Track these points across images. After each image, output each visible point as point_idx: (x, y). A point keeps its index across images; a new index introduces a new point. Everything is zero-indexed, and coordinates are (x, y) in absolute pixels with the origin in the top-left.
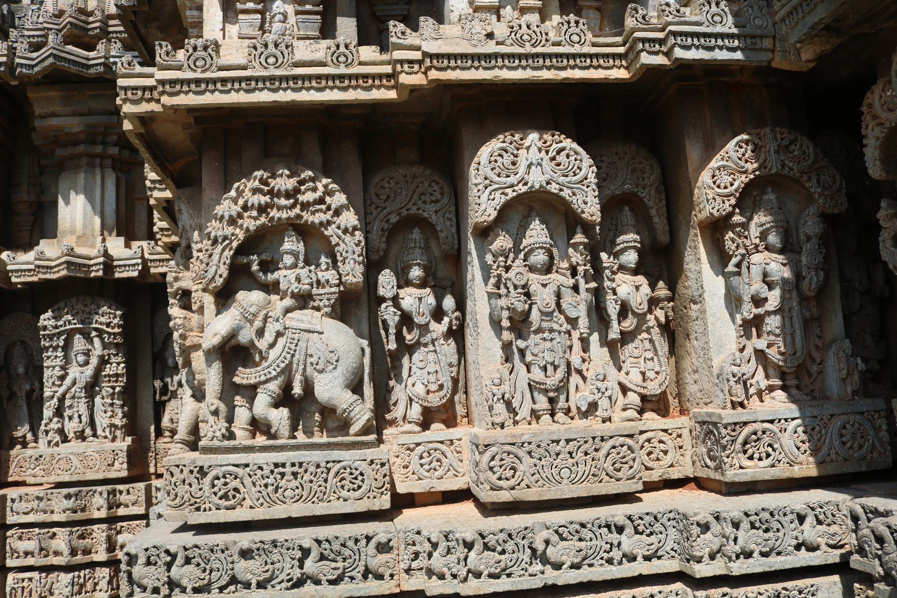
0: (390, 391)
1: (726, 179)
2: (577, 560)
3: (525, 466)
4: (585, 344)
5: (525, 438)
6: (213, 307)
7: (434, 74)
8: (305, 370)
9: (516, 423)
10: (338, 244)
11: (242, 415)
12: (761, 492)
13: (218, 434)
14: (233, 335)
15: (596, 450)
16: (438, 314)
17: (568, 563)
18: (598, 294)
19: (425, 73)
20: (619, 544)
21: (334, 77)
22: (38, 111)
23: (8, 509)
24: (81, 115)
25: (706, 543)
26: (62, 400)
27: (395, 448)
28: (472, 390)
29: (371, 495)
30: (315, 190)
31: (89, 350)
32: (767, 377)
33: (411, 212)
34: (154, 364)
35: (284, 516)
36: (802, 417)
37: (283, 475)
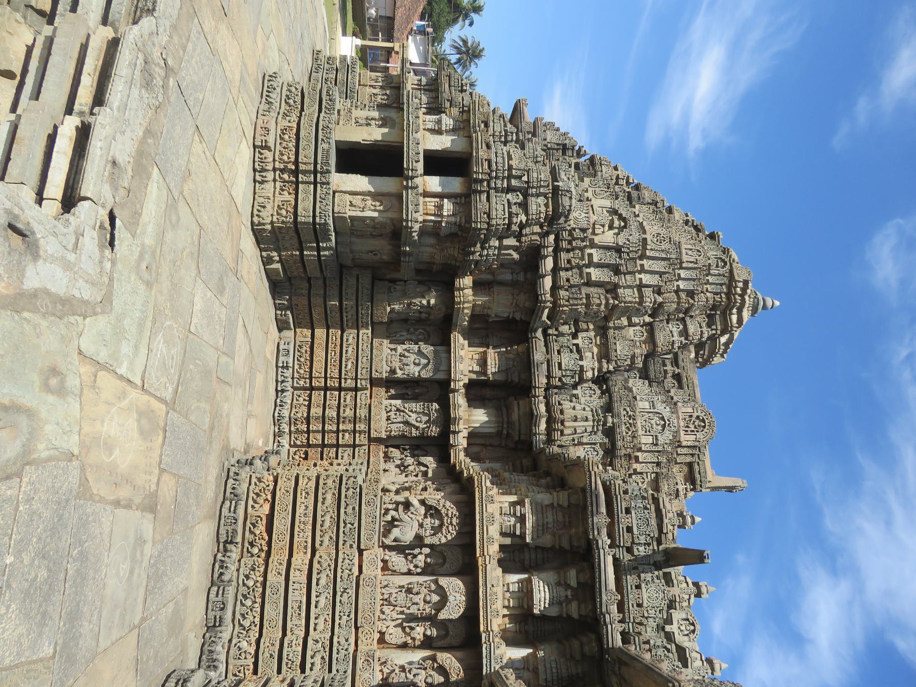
1: (448, 661)
4: (402, 613)
7: (480, 568)
11: (391, 506)
14: (412, 505)
16: (416, 566)
25: (343, 641)
26: (403, 411)
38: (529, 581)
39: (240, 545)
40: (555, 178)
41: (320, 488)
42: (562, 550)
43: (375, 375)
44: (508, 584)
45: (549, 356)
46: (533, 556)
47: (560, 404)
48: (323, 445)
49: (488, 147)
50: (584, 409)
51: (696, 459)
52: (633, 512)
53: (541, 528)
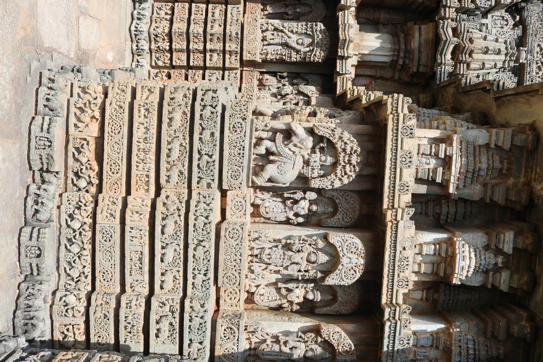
0: (268, 192)
1: (336, 336)
2: (196, 257)
3: (233, 242)
4: (278, 272)
5: (243, 243)
6: (308, 126)
7: (389, 224)
8: (279, 161)
9: (250, 241)
10: (327, 179)
12: (211, 332)
13: (258, 126)
14: (295, 134)
15: (236, 270)
16: (297, 215)
17: (195, 254)
18: (296, 280)
19: (391, 221)
20: (200, 274)
21: (394, 184)
22: (423, 27)
23: (234, 6)
24: (419, 48)
25: (197, 307)
26: (282, 31)
27: (245, 192)
28: (264, 225)
29: (229, 182)
30: (350, 171)
31: (304, 45)
32: (255, 343)
33: (340, 209)
34: (295, 73)
35: (224, 148)
36: (238, 353)
37: (240, 149)
38: (450, 243)
39: (62, 175)
42: (493, 204)
44: (421, 245)
46: (452, 210)
50: (497, 40)
53: (469, 175)
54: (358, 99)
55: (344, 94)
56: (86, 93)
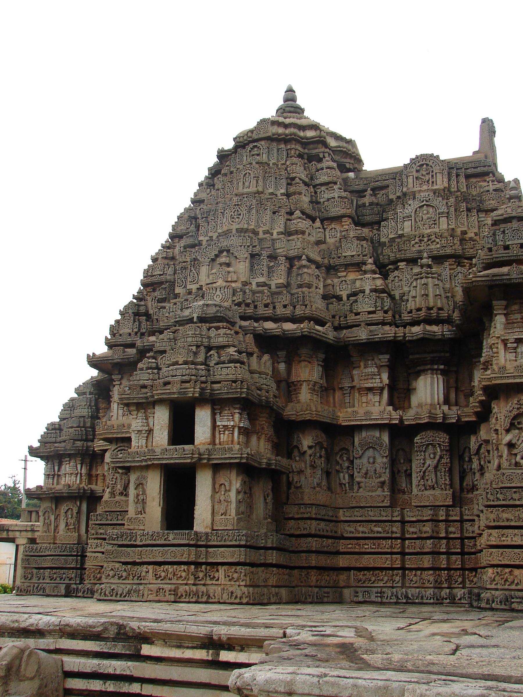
26: (424, 472)
40: (190, 321)
41: (498, 524)
43: (387, 503)
45: (363, 324)
47: (411, 312)
48: (463, 553)
49: (166, 384)
51: (462, 172)
52: (508, 243)
54: (481, 402)
55: (476, 414)
56: (494, 580)
